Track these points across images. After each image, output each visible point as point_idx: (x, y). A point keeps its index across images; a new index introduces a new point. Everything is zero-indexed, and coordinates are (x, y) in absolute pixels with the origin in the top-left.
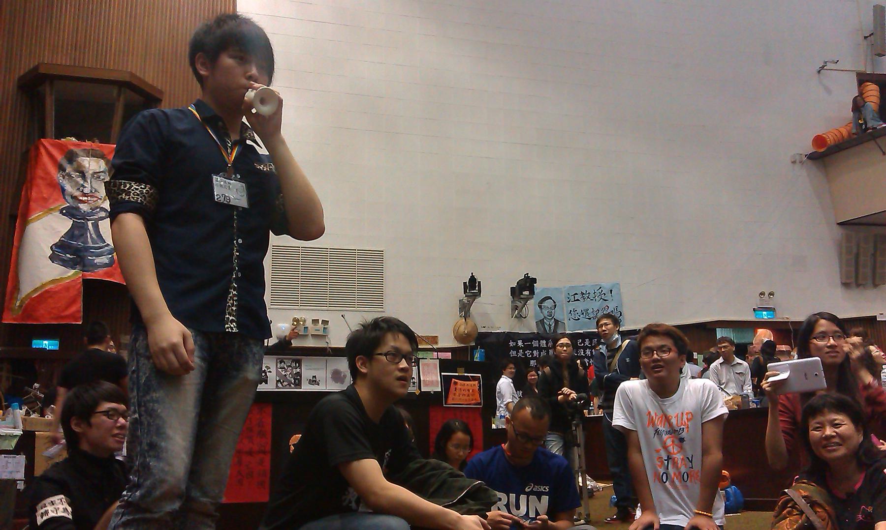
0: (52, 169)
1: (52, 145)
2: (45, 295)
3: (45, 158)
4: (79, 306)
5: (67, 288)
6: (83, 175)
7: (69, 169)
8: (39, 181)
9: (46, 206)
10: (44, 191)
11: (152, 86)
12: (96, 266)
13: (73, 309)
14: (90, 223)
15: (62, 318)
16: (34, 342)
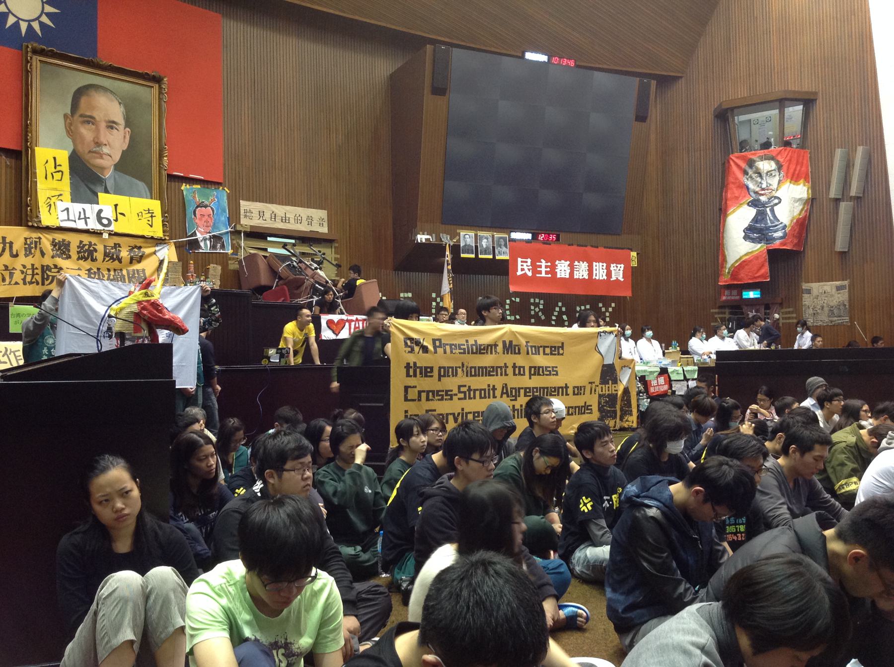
0: (739, 174)
1: (738, 158)
2: (743, 264)
3: (734, 168)
4: (766, 269)
5: (757, 257)
6: (760, 176)
7: (750, 172)
8: (731, 186)
9: (737, 201)
10: (735, 191)
11: (807, 93)
12: (775, 239)
13: (762, 271)
14: (768, 209)
15: (755, 278)
16: (744, 293)
